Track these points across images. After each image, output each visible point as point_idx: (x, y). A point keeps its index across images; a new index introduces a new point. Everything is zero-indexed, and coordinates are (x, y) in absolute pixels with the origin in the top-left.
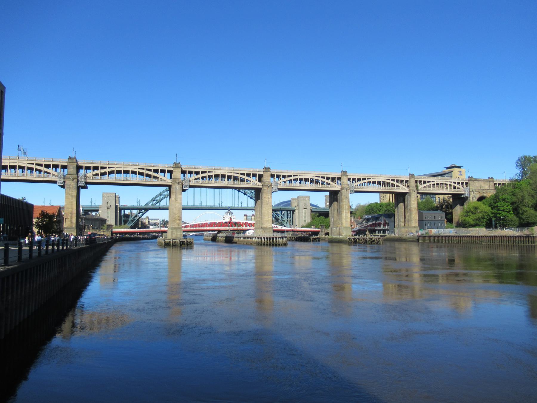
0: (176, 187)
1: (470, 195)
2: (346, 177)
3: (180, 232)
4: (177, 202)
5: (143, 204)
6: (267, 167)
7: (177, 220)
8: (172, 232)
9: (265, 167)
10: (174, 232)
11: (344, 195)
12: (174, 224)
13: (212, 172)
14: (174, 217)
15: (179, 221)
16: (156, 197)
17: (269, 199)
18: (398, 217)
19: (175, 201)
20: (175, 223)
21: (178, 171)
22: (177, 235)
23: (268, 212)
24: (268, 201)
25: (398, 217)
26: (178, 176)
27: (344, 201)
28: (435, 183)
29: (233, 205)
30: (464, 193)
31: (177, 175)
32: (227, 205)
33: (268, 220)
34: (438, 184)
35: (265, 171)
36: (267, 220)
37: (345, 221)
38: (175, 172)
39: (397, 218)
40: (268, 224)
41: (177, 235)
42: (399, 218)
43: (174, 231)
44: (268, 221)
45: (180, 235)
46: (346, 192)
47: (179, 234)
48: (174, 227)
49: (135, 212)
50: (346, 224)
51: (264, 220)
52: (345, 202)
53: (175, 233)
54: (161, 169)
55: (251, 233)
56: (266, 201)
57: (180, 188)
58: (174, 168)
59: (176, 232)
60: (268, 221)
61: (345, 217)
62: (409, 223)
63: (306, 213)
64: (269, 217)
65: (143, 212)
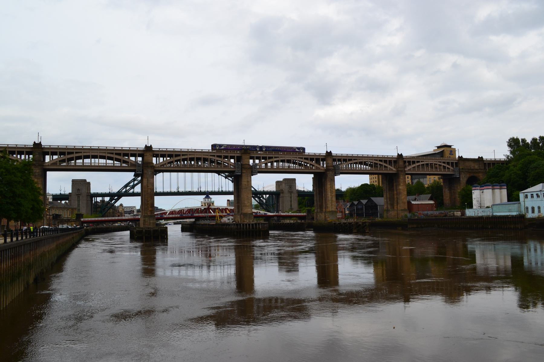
1: (460, 175)
2: (330, 158)
4: (149, 187)
5: (115, 190)
8: (144, 220)
10: (146, 220)
15: (152, 208)
16: (130, 183)
17: (249, 183)
21: (149, 155)
23: (248, 196)
24: (248, 185)
28: (425, 163)
29: (192, 190)
32: (192, 190)
34: (427, 164)
37: (331, 204)
38: (147, 156)
40: (248, 210)
45: (153, 223)
47: (152, 222)
49: (107, 199)
50: (332, 208)
53: (147, 221)
54: (131, 153)
56: (246, 185)
58: (145, 152)
61: (331, 200)
63: (292, 197)
65: (115, 199)
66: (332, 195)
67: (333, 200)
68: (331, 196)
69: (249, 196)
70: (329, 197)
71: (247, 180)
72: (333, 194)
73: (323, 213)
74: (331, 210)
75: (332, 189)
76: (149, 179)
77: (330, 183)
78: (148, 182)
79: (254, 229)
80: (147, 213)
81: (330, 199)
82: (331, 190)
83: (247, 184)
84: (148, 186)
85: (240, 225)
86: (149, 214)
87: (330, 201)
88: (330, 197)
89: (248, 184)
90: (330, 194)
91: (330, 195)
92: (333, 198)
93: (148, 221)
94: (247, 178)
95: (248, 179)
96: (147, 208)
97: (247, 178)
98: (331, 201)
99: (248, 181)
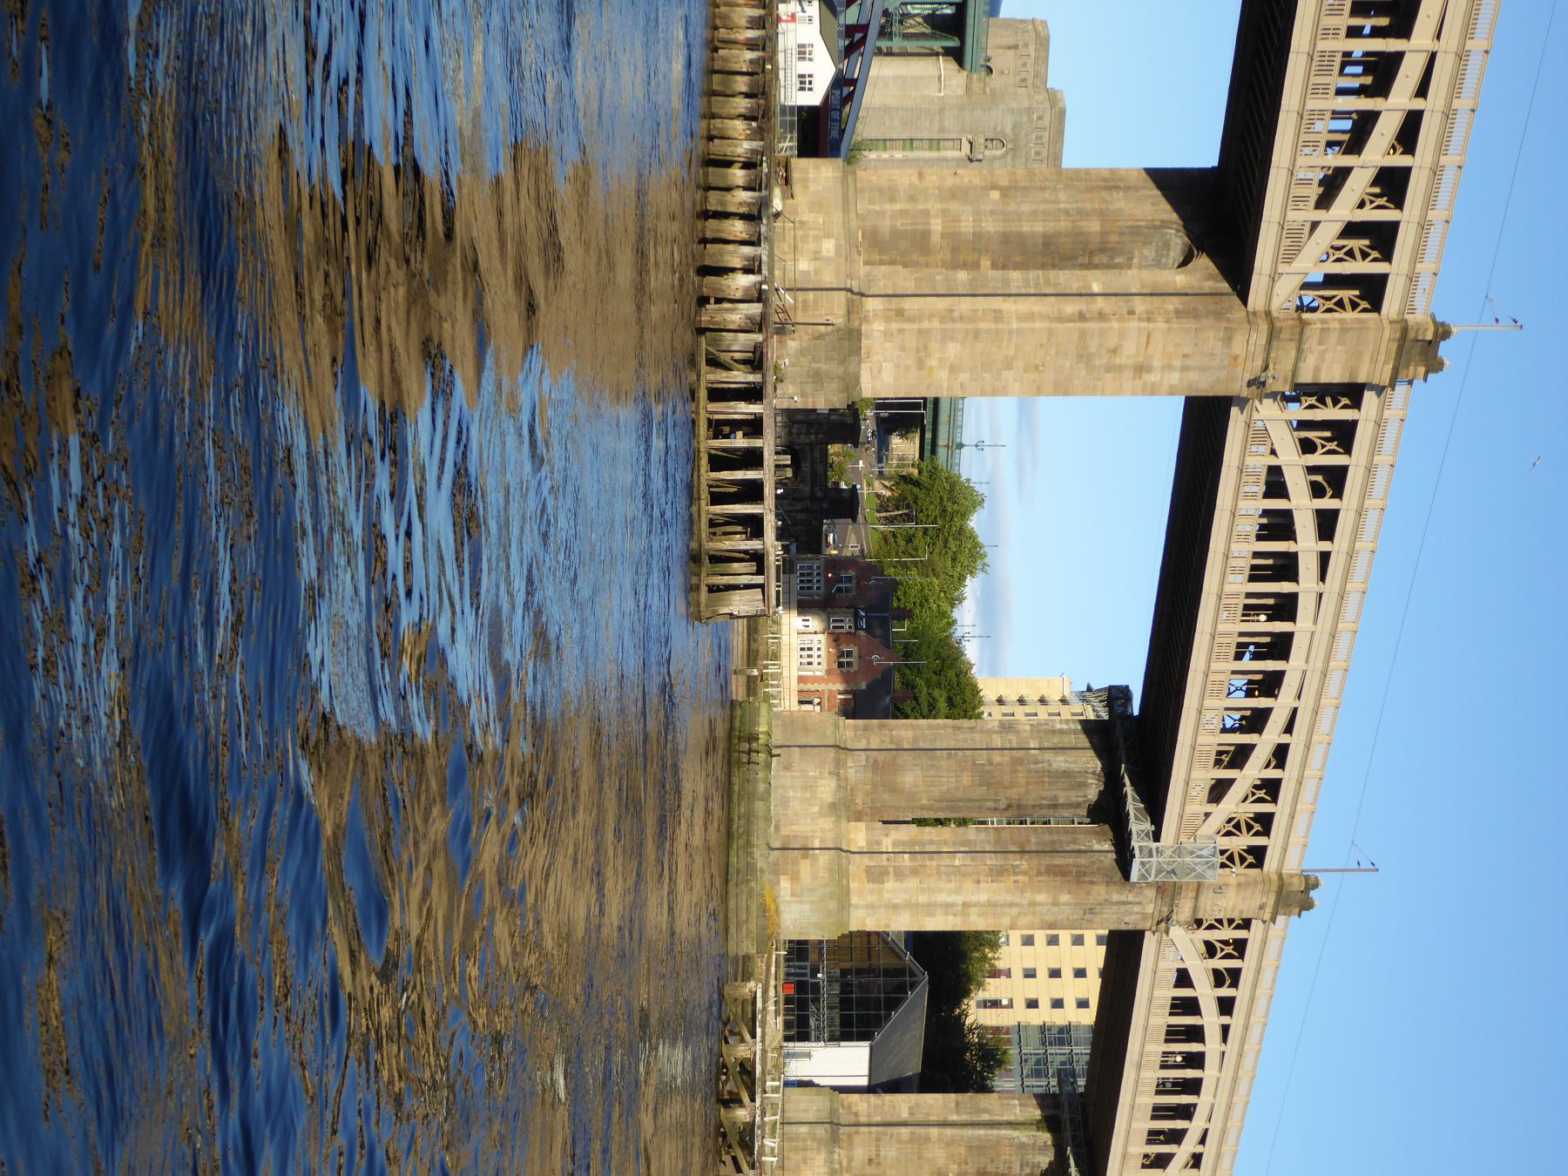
6: (1445, 350)
9: (1443, 332)
11: (1115, 897)
17: (1128, 374)
23: (1009, 367)
27: (1065, 898)
33: (934, 363)
35: (1412, 335)
36: (928, 355)
37: (897, 901)
44: (921, 364)
46: (1136, 909)
50: (870, 906)
52: (1055, 904)
55: (803, 67)
60: (921, 364)
64: (953, 369)
66: (974, 910)
67: (932, 914)
68: (965, 905)
70: (958, 891)
71: (1157, 363)
72: (981, 915)
73: (827, 823)
74: (854, 900)
75: (1015, 911)
77: (1067, 904)
79: (713, 407)
81: (942, 898)
82: (1011, 905)
83: (1117, 361)
85: (753, 394)
87: (923, 899)
88: (959, 899)
89: (1120, 368)
90: (983, 897)
91: (974, 898)
92: (946, 914)
94: (1177, 363)
95: (1168, 367)
97: (1177, 363)
98: (929, 905)
99: (1149, 369)
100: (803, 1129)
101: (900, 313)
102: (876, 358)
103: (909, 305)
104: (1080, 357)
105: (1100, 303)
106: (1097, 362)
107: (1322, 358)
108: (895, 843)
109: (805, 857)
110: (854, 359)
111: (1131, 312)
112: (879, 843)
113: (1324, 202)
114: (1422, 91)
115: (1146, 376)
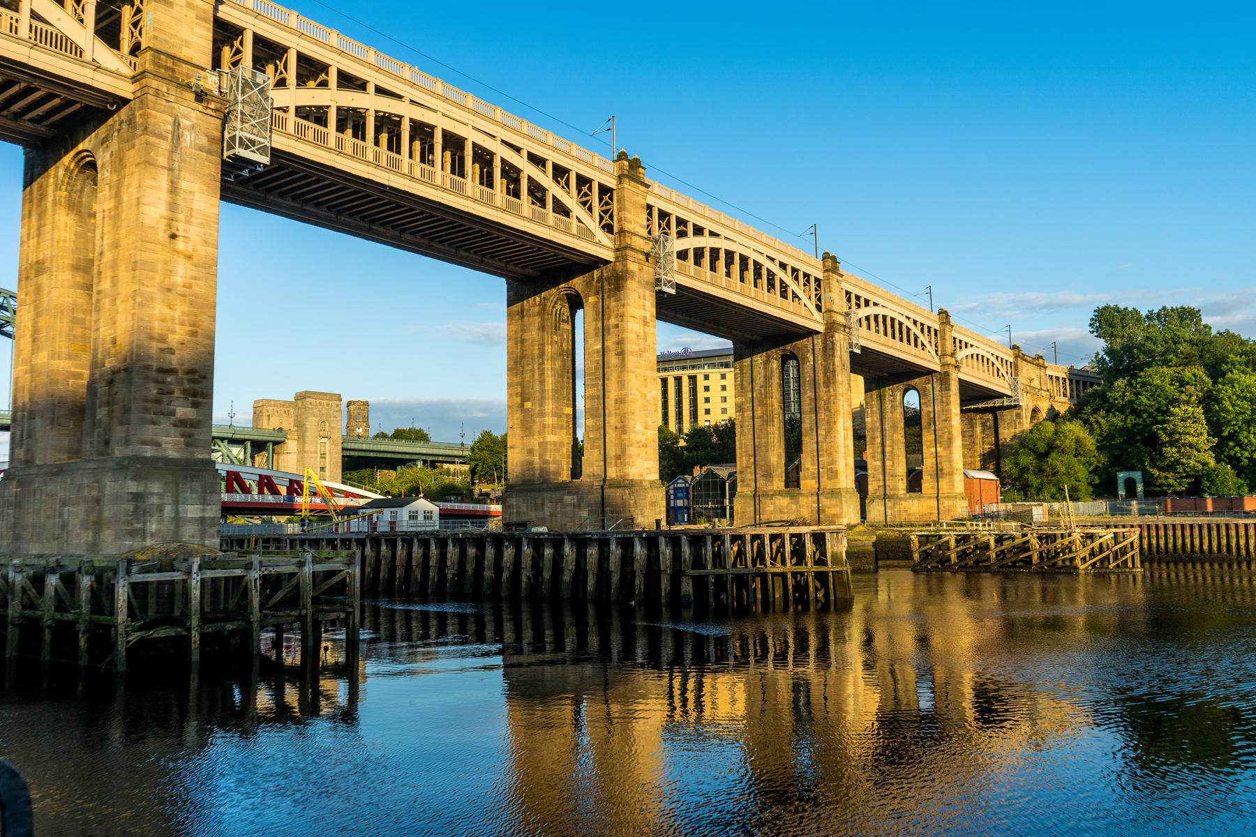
0: (177, 124)
3: (204, 502)
4: (180, 244)
7: (177, 394)
12: (149, 432)
13: (400, 97)
14: (154, 374)
15: (195, 405)
18: (884, 463)
19: (163, 236)
20: (165, 424)
22: (178, 521)
23: (645, 395)
25: (884, 463)
26: (187, 44)
30: (1009, 393)
31: (186, 35)
33: (644, 438)
39: (879, 463)
41: (178, 521)
42: (888, 463)
43: (155, 487)
45: (202, 521)
47: (192, 511)
48: (149, 452)
51: (632, 436)
53: (160, 509)
57: (204, 141)
59: (168, 499)
62: (944, 483)
63: (328, 456)
69: (649, 396)
71: (642, 313)
73: (802, 500)
76: (183, 185)
78: (173, 206)
80: (157, 444)
83: (642, 335)
84: (173, 236)
86: (172, 454)
89: (645, 333)
93: (168, 510)
96: (158, 401)
99: (645, 318)
100: (889, 512)
101: (618, 457)
102: (643, 472)
103: (612, 452)
104: (640, 355)
105: (610, 343)
106: (642, 346)
107: (636, 222)
108: (813, 465)
109: (824, 511)
110: (644, 483)
111: (617, 326)
112: (814, 473)
113: (566, 212)
114: (518, 150)
115: (648, 320)
